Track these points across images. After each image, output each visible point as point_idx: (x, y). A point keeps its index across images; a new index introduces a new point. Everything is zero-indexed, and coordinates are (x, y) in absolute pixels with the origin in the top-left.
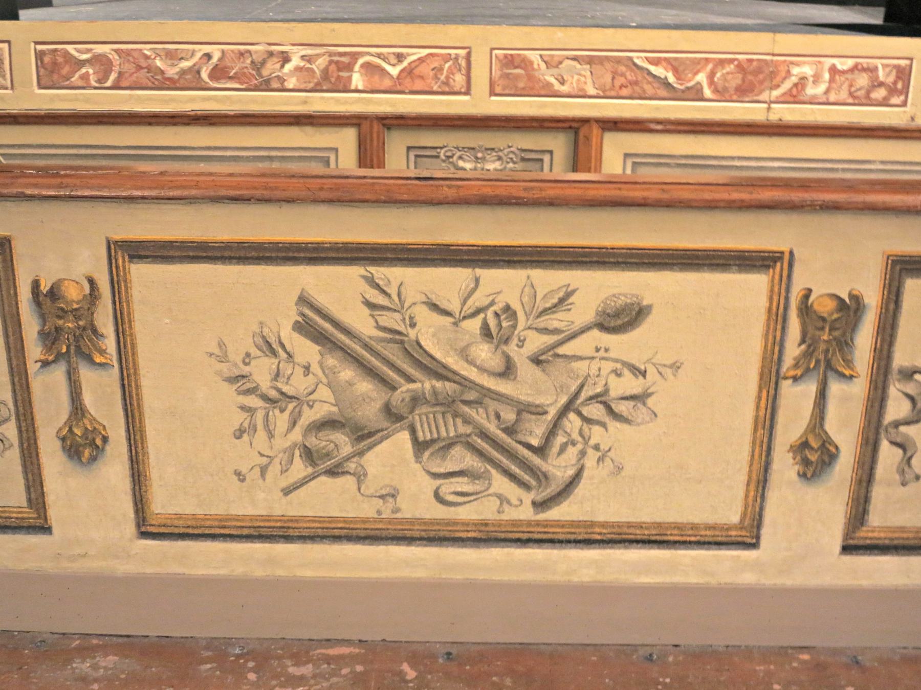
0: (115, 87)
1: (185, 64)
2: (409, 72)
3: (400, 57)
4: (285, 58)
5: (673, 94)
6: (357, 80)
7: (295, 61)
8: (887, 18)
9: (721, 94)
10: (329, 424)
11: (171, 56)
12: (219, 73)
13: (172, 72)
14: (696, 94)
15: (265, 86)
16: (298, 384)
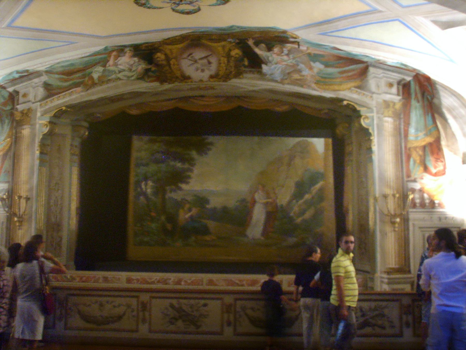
0: (140, 284)
1: (152, 280)
2: (192, 282)
3: (190, 279)
4: (170, 279)
5: (238, 285)
6: (183, 283)
7: (172, 280)
9: (249, 285)
10: (172, 318)
11: (151, 279)
12: (159, 282)
13: (150, 281)
14: (243, 285)
15: (166, 284)
16: (169, 313)
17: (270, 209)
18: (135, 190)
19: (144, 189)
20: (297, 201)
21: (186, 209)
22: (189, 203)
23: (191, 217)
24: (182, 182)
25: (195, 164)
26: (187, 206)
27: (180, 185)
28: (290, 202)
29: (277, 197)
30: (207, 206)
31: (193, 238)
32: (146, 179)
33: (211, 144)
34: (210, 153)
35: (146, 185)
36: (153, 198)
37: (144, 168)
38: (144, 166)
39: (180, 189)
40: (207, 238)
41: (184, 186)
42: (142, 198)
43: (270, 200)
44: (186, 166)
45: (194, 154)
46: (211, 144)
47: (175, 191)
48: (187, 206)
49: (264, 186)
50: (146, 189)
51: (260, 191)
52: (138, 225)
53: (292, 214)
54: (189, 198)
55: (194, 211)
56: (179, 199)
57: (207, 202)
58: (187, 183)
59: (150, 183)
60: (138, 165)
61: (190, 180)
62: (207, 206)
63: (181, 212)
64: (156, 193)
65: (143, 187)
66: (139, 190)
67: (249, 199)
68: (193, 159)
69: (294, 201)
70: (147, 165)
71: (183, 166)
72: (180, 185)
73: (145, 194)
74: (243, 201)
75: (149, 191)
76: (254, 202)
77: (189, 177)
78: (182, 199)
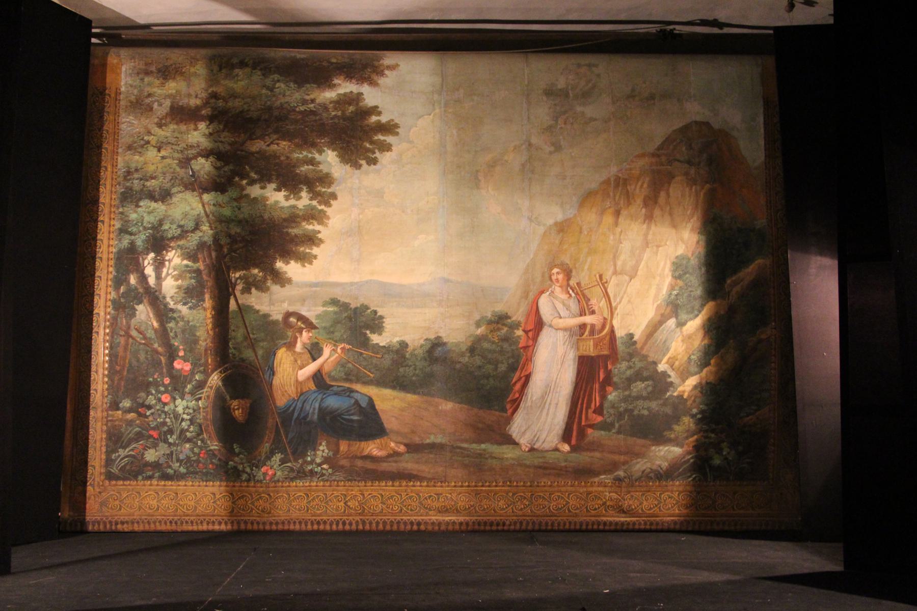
8: (845, 568)
17: (589, 348)
18: (119, 281)
19: (152, 281)
20: (681, 324)
21: (299, 347)
22: (310, 326)
23: (318, 377)
24: (287, 254)
25: (334, 196)
26: (305, 337)
27: (279, 264)
28: (654, 327)
29: (612, 311)
30: (375, 339)
31: (323, 450)
32: (158, 244)
33: (389, 128)
34: (385, 158)
35: (159, 265)
36: (184, 310)
37: (153, 205)
38: (152, 197)
39: (280, 279)
40: (373, 448)
41: (291, 269)
42: (143, 312)
43: (588, 319)
44: (304, 201)
45: (330, 160)
46: (389, 128)
47: (261, 286)
48: (305, 337)
49: (568, 274)
50: (159, 278)
51: (558, 290)
52: (126, 403)
53: (662, 367)
54: (311, 312)
55: (329, 356)
56: (277, 316)
57: (376, 324)
58: (305, 259)
59: (174, 259)
60: (129, 197)
61: (315, 251)
62: (375, 339)
63: (283, 359)
64: (191, 294)
65: (149, 271)
66: (133, 280)
67: (519, 315)
68: (326, 179)
69: (672, 322)
70: (164, 196)
71: (292, 202)
72: (279, 264)
73: (154, 298)
74: (501, 319)
75: (170, 287)
76: (539, 325)
77: (312, 239)
78: (288, 315)
